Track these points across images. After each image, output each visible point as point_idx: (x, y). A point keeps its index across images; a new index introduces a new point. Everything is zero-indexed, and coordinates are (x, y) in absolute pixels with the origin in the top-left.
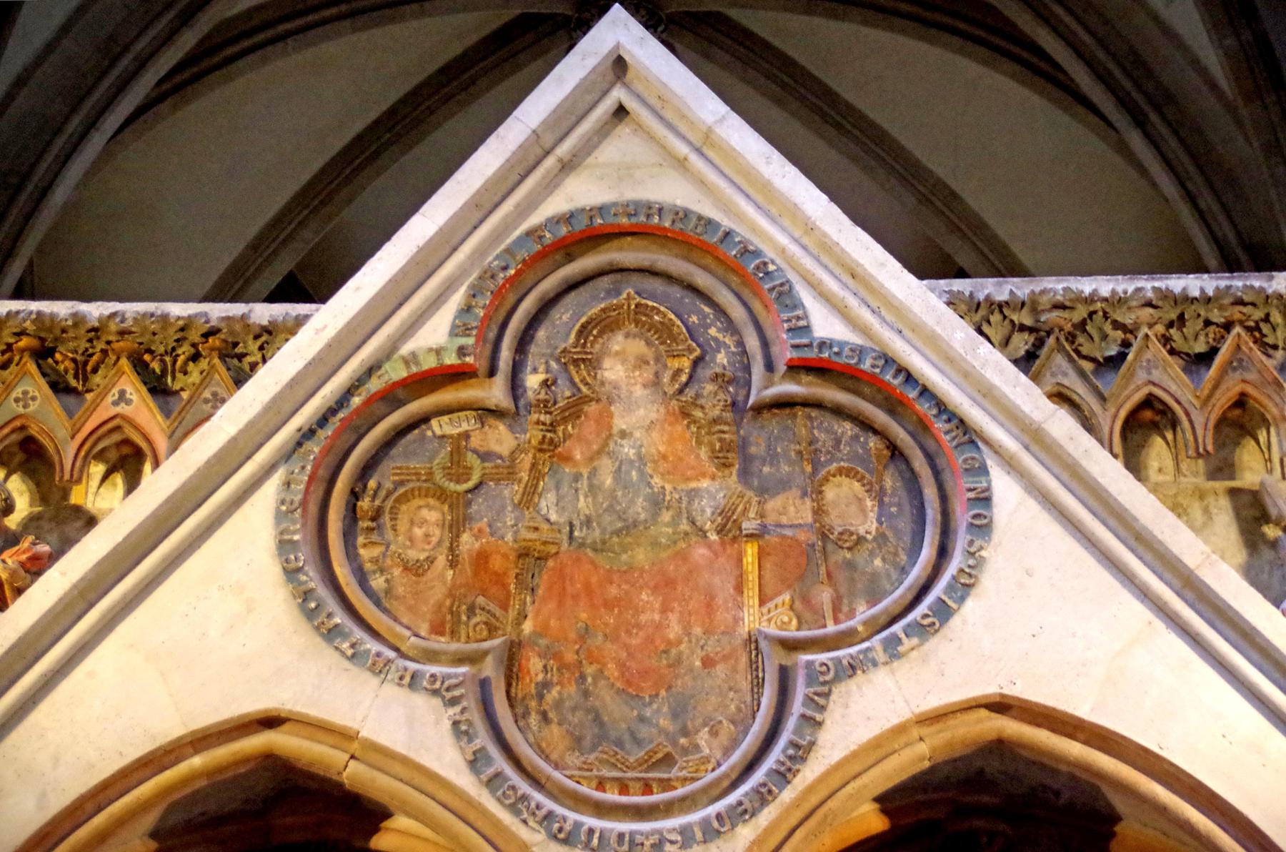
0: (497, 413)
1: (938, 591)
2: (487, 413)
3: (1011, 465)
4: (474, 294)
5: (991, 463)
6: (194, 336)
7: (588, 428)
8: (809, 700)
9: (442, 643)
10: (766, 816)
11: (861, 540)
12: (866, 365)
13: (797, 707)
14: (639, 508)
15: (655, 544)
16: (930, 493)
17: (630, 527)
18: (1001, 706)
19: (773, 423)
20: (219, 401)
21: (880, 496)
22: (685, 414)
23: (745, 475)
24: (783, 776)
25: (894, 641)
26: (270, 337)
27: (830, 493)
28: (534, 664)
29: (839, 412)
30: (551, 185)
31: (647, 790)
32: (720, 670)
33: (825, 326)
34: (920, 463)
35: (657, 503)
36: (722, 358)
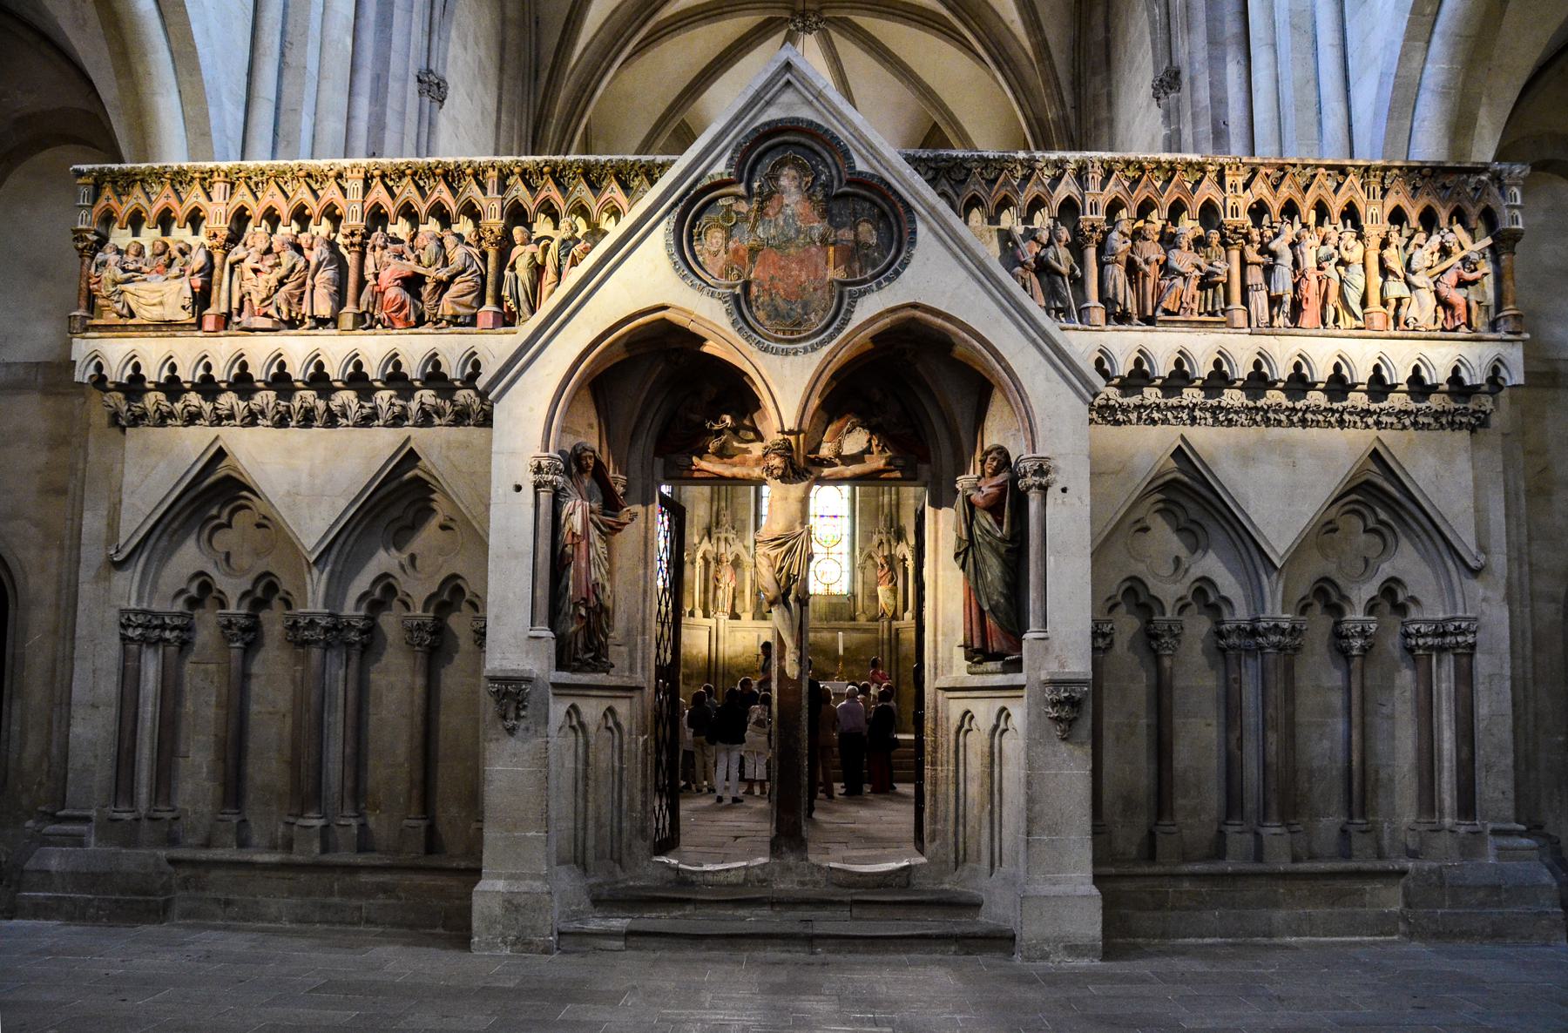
0: (742, 197)
1: (896, 265)
2: (738, 197)
3: (923, 219)
4: (735, 151)
5: (917, 218)
6: (636, 168)
7: (775, 203)
8: (849, 304)
9: (723, 281)
10: (834, 342)
11: (870, 246)
12: (875, 181)
13: (845, 306)
14: (792, 233)
15: (797, 246)
16: (895, 229)
17: (789, 240)
18: (915, 306)
19: (841, 203)
20: (645, 192)
21: (877, 229)
22: (809, 198)
23: (830, 222)
24: (839, 330)
25: (880, 283)
26: (663, 167)
27: (860, 228)
28: (754, 289)
29: (865, 198)
30: (762, 111)
31: (792, 334)
32: (819, 292)
33: (860, 166)
34: (892, 219)
35: (798, 231)
36: (823, 177)
